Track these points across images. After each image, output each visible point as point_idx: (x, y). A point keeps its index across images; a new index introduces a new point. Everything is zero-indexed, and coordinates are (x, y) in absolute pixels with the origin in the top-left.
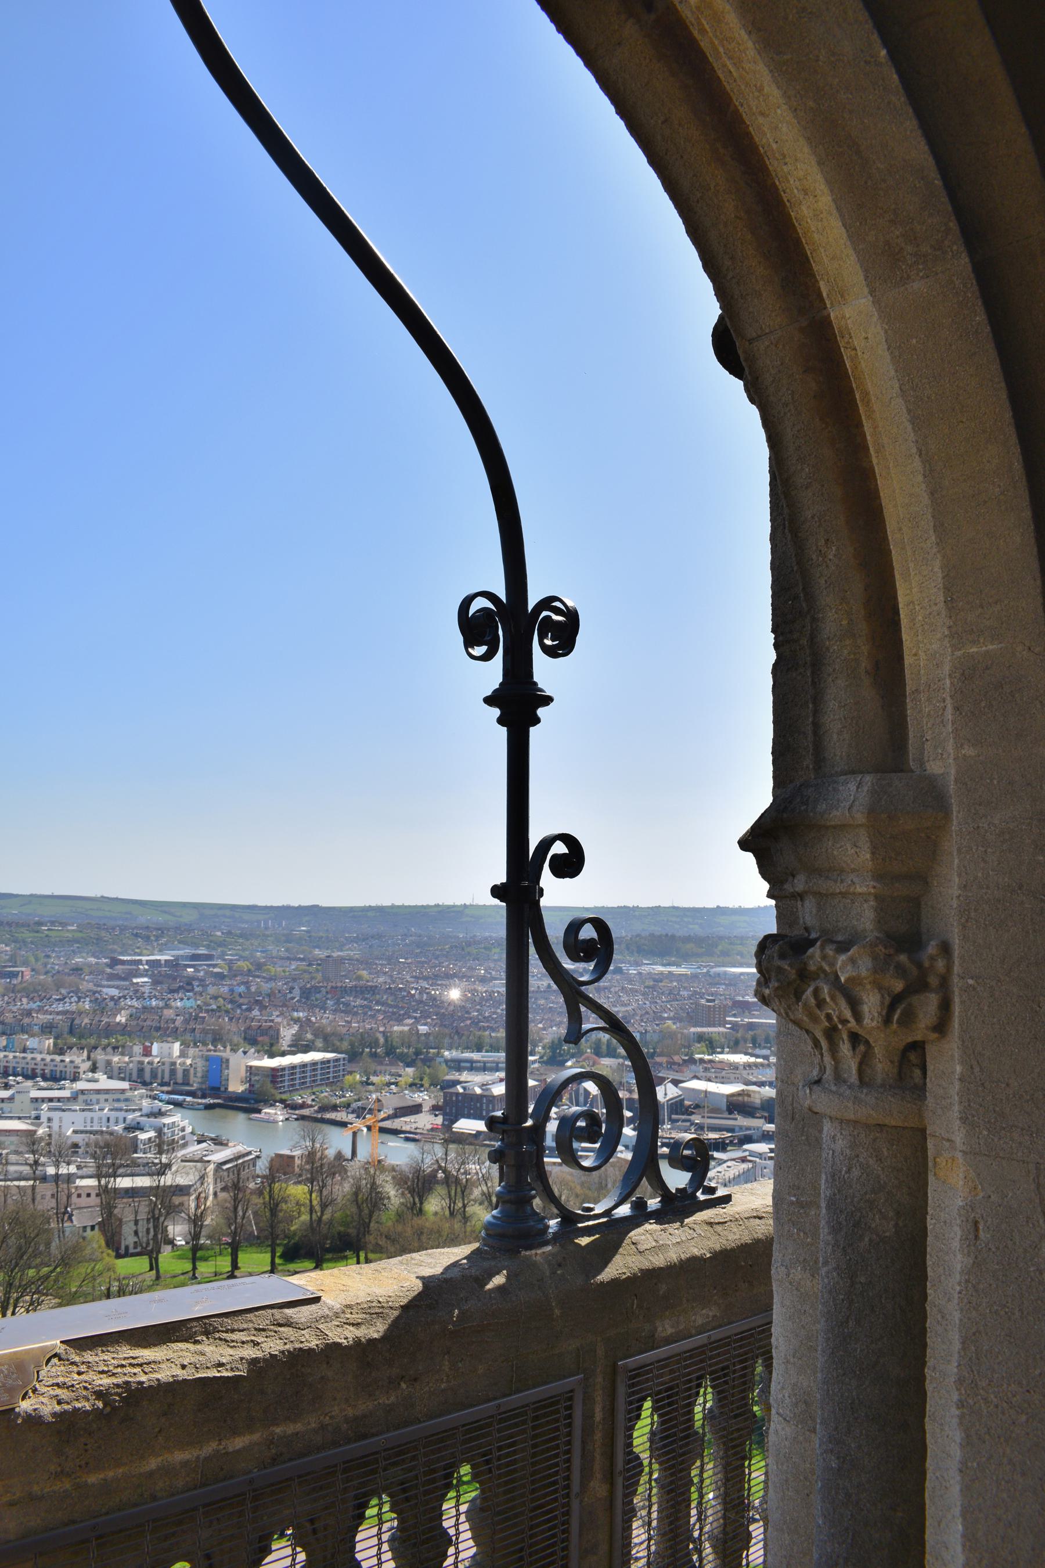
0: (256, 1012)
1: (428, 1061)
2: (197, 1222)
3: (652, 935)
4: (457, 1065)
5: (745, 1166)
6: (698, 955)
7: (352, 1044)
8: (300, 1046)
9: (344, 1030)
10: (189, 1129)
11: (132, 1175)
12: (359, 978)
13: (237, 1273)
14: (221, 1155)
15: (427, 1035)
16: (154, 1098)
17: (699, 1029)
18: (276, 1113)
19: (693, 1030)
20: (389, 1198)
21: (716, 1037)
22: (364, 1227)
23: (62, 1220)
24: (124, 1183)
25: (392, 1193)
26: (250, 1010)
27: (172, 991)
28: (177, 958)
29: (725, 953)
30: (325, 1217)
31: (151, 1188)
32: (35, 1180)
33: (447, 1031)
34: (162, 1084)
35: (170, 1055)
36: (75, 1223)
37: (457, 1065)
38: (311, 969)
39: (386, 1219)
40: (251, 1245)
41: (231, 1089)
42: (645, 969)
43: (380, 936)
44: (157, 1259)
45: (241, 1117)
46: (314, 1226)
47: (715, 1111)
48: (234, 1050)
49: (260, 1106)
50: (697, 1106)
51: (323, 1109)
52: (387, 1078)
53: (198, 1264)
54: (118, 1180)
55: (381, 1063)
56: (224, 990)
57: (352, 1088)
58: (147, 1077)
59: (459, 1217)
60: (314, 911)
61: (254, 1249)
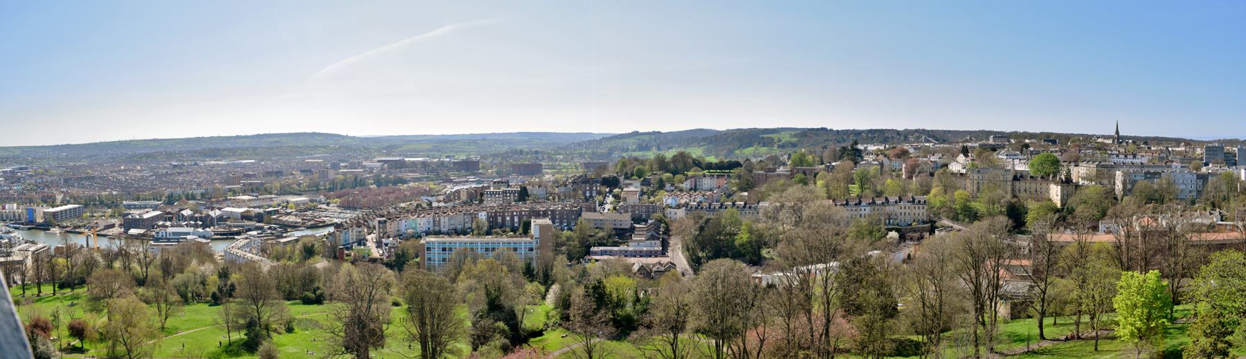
0: (46, 190)
1: (116, 206)
2: (23, 274)
3: (210, 149)
4: (129, 207)
5: (247, 241)
6: (228, 156)
7: (85, 201)
8: (63, 203)
9: (82, 195)
10: (21, 238)
12: (87, 173)
14: (33, 249)
15: (116, 195)
16: (7, 226)
17: (229, 187)
18: (56, 230)
19: (227, 187)
21: (236, 189)
22: (89, 274)
25: (101, 260)
26: (43, 189)
27: (12, 183)
28: (14, 169)
29: (241, 155)
30: (74, 271)
33: (125, 193)
34: (10, 221)
35: (13, 209)
37: (129, 207)
38: (68, 171)
39: (97, 272)
40: (46, 283)
41: (37, 221)
42: (207, 163)
43: (95, 156)
45: (42, 233)
46: (69, 275)
47: (236, 219)
48: (38, 206)
49: (50, 227)
50: (229, 218)
51: (75, 228)
52: (101, 214)
53: (26, 291)
55: (98, 208)
56: (33, 181)
57: (86, 218)
58: (5, 218)
59: (127, 269)
60: (68, 146)
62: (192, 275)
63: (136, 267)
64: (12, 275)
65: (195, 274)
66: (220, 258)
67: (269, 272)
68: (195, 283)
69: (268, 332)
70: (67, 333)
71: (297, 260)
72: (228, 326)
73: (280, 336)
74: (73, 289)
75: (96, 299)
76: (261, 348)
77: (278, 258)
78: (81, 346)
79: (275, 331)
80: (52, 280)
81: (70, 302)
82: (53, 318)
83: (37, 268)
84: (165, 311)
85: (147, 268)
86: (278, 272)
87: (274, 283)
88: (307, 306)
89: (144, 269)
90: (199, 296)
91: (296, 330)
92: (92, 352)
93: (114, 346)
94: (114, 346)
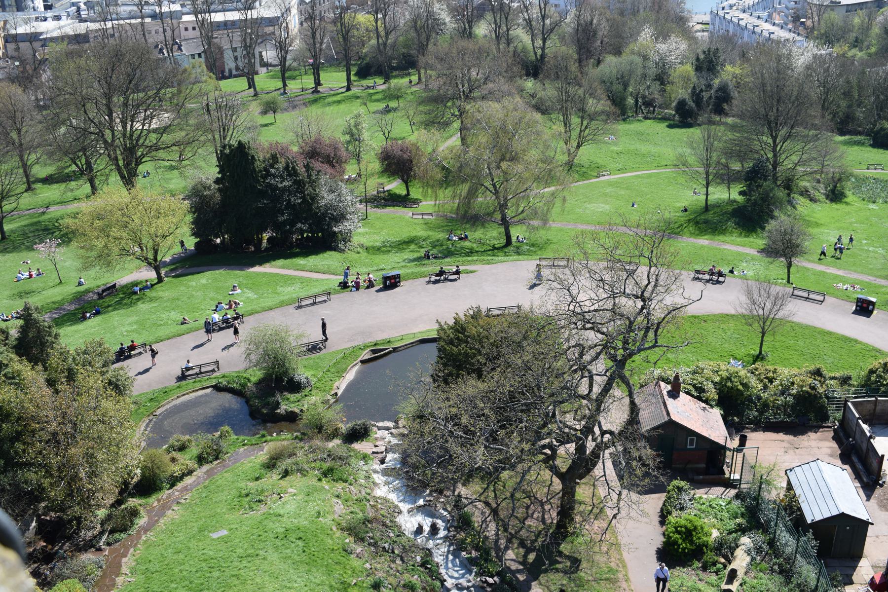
2: (282, 47)
11: (224, 11)
13: (320, 89)
20: (444, 24)
22: (423, 48)
23: (172, 50)
24: (218, 17)
31: (240, 20)
32: (142, 17)
36: (184, 52)
39: (441, 44)
44: (253, 79)
46: (381, 48)
53: (287, 82)
54: (213, 15)
59: (503, 40)
61: (333, 69)
62: (638, 60)
63: (522, 36)
64: (257, 50)
65: (645, 58)
66: (699, 27)
67: (808, 67)
68: (644, 76)
69: (789, 195)
70: (375, 165)
71: (873, 50)
72: (707, 174)
73: (814, 205)
74: (387, 78)
75: (437, 100)
76: (771, 225)
77: (828, 39)
78: (404, 192)
79: (805, 193)
80: (344, 60)
81: (381, 106)
82: (348, 137)
83: (312, 35)
84: (578, 130)
85: (544, 40)
86: (827, 70)
87: (815, 93)
88: (881, 151)
89: (539, 42)
90: (649, 104)
91: (850, 197)
92: (427, 205)
93: (472, 194)
94: (472, 194)
